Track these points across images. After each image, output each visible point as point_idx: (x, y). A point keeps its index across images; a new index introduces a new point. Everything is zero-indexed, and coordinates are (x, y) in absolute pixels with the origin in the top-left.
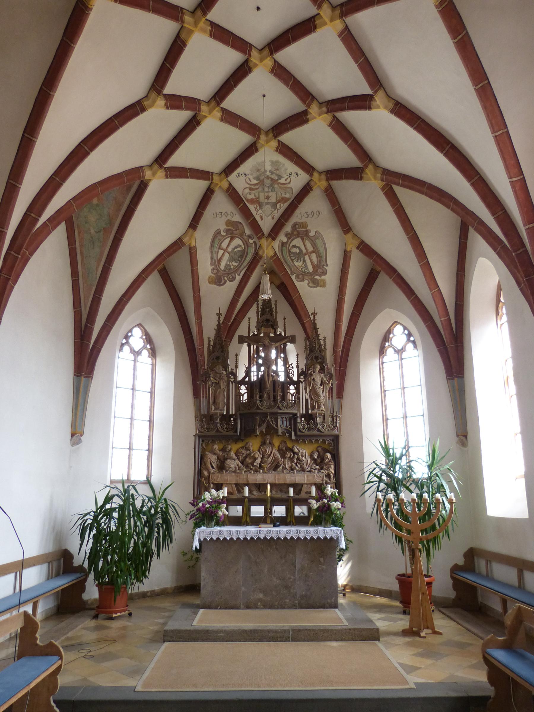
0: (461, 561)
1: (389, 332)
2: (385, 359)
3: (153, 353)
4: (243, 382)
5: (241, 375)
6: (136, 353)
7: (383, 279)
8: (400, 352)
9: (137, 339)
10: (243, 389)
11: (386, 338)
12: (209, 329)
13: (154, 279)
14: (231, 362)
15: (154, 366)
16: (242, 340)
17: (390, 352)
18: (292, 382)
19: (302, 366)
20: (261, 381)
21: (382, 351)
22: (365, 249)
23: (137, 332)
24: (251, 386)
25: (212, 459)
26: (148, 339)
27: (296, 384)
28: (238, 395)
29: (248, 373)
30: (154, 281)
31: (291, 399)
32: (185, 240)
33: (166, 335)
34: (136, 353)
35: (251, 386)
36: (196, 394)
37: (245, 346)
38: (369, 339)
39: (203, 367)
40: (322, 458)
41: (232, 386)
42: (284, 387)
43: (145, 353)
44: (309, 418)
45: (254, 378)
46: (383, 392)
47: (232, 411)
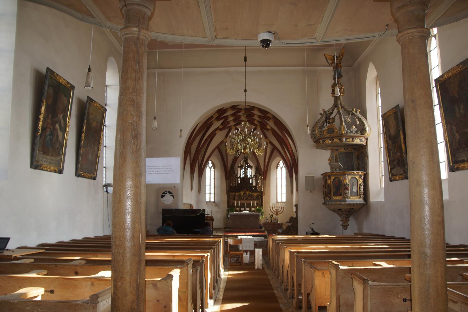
0: (288, 221)
1: (279, 162)
2: (278, 169)
3: (214, 168)
4: (239, 178)
5: (239, 176)
6: (210, 168)
7: (275, 151)
8: (281, 168)
9: (210, 164)
10: (239, 180)
11: (278, 164)
12: (230, 159)
13: (217, 151)
14: (236, 173)
15: (215, 171)
16: (239, 167)
17: (279, 168)
18: (251, 178)
19: (254, 174)
20: (243, 178)
21: (277, 167)
22: (271, 143)
23: (210, 162)
24: (241, 179)
25: (231, 197)
26: (213, 164)
27: (252, 178)
28: (238, 182)
29: (240, 175)
30: (217, 151)
31: (251, 182)
32: (224, 141)
33: (218, 163)
34: (210, 168)
35: (241, 179)
36: (226, 179)
37: (240, 168)
38: (274, 164)
39: (228, 172)
40: (258, 197)
41: (236, 179)
42: (250, 178)
43: (212, 168)
44: (256, 187)
45: (242, 177)
46: (277, 178)
47: (236, 185)
